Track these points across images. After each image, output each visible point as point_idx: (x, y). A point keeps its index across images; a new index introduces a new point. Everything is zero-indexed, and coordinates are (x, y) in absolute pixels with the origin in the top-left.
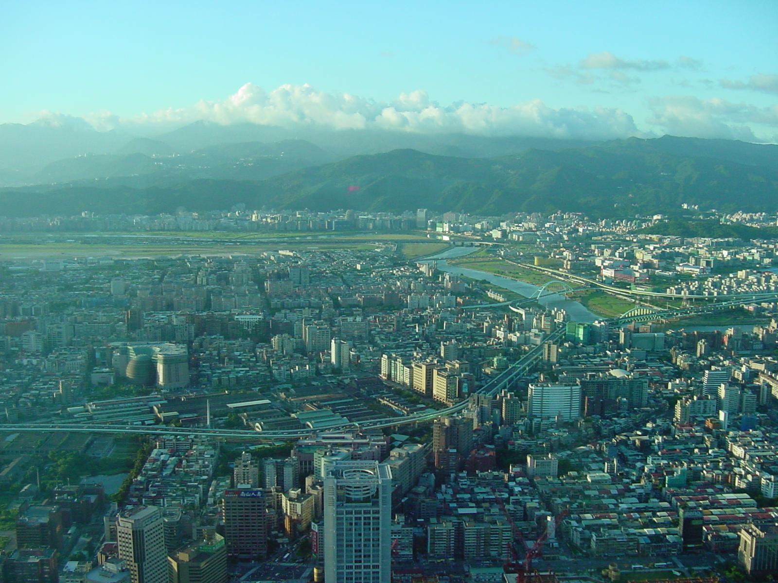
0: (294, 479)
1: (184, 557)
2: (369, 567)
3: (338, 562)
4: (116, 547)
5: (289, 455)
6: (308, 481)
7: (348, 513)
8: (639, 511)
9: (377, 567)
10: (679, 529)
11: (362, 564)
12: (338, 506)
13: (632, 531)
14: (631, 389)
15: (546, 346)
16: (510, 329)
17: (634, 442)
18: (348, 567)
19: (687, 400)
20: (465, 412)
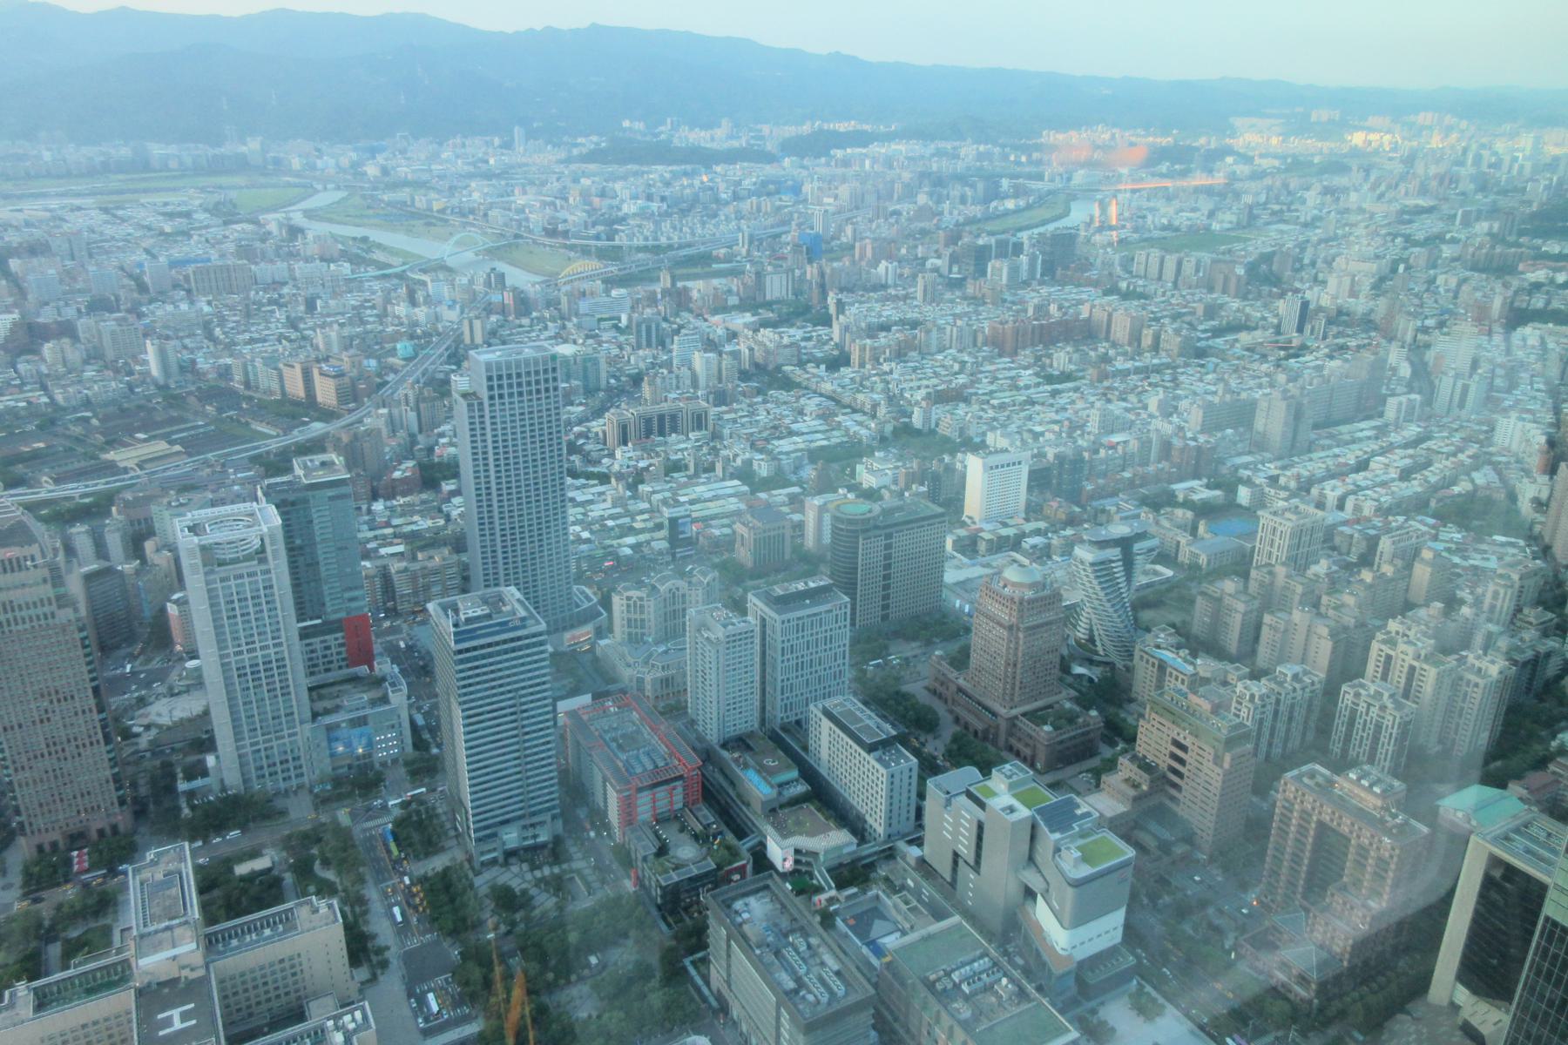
0: (125, 549)
2: (267, 647)
3: (220, 649)
5: (108, 514)
6: (149, 546)
7: (222, 580)
8: (612, 517)
9: (280, 644)
10: (664, 533)
11: (257, 645)
12: (206, 574)
13: (608, 542)
14: (585, 370)
15: (466, 323)
16: (413, 302)
18: (236, 654)
19: (656, 375)
20: (367, 421)
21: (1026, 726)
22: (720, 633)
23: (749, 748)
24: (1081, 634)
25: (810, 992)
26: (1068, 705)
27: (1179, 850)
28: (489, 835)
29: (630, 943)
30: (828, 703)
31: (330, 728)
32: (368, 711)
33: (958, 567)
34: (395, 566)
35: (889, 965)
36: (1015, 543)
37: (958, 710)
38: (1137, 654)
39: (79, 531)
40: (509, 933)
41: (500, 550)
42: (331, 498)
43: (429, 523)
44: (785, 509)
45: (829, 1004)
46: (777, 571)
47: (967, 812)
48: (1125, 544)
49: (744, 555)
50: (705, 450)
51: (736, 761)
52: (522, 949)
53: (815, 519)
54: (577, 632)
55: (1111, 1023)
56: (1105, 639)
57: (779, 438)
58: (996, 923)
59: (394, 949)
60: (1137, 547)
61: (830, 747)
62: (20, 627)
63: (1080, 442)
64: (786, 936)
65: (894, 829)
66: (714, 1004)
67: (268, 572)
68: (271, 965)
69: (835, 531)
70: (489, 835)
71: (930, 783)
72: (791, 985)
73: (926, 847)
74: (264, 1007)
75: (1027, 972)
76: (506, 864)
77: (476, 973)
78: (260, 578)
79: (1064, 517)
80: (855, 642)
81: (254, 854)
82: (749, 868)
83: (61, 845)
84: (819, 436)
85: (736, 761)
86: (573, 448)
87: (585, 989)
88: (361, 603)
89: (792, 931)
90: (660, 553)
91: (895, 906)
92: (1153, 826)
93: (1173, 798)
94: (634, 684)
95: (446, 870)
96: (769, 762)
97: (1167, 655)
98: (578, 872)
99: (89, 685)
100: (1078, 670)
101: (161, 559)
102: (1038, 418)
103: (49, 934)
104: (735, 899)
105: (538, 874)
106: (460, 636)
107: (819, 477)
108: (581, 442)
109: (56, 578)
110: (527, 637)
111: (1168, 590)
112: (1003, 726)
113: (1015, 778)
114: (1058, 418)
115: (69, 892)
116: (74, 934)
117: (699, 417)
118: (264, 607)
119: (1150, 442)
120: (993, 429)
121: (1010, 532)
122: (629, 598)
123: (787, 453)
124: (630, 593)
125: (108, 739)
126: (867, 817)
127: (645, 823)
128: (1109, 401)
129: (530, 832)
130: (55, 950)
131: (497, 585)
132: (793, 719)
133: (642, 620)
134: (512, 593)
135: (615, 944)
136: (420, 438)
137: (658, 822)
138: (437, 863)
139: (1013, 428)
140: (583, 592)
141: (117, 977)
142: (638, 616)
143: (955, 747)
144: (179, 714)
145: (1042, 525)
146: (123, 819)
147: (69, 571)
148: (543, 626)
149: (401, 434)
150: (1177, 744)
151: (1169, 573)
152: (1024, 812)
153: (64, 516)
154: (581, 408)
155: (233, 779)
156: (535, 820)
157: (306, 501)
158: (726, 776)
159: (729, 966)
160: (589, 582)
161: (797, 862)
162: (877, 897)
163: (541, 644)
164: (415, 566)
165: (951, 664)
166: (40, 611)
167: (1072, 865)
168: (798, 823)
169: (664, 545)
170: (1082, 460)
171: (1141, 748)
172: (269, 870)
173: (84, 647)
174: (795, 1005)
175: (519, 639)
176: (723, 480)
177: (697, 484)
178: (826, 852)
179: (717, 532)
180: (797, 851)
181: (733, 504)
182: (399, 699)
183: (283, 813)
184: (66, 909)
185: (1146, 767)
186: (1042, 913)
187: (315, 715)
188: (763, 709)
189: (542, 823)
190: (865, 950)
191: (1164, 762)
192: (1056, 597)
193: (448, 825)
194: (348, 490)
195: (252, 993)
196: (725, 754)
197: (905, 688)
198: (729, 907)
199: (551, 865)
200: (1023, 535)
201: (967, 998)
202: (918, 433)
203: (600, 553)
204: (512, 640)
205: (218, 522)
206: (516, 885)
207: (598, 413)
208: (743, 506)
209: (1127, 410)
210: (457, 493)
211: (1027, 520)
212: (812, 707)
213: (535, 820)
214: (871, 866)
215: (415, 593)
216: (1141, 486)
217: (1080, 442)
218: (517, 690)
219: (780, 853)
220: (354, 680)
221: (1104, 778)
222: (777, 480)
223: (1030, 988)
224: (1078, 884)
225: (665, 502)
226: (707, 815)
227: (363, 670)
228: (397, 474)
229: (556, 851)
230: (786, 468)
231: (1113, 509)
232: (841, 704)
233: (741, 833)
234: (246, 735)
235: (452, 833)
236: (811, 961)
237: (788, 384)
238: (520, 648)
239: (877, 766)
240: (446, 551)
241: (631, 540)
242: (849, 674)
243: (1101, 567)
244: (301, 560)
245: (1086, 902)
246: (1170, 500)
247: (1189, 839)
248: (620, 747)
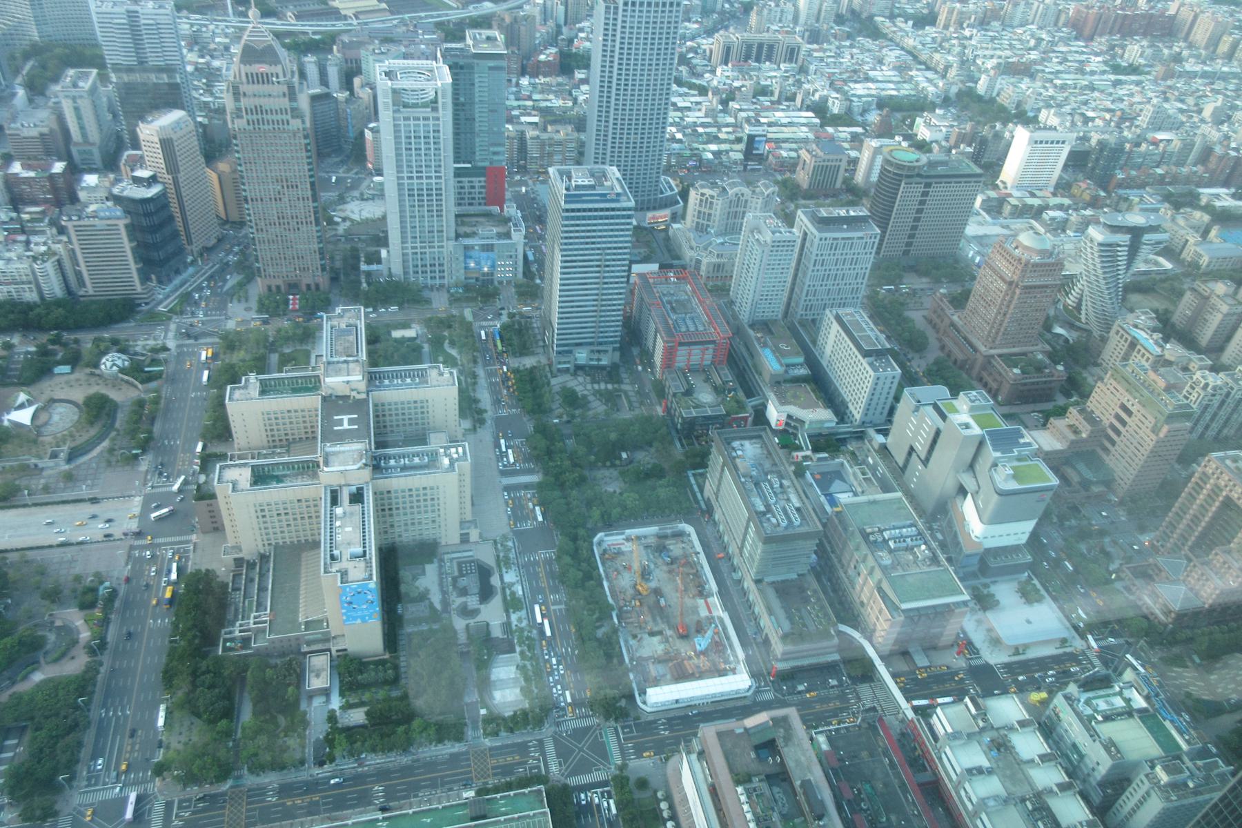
0: (341, 82)
1: (223, 166)
2: (430, 178)
4: (142, 157)
5: (331, 51)
6: (357, 81)
7: (406, 119)
8: (703, 125)
9: (440, 177)
10: (742, 146)
11: (424, 175)
12: (394, 112)
13: (696, 145)
17: (705, 51)
19: (764, 6)
20: (526, 7)
21: (999, 364)
22: (768, 237)
23: (771, 332)
24: (1071, 301)
25: (774, 516)
26: (1040, 356)
27: (1096, 489)
28: (566, 350)
29: (653, 450)
30: (841, 311)
31: (467, 248)
32: (495, 242)
33: (980, 224)
34: (531, 133)
35: (838, 513)
36: (1037, 213)
37: (947, 340)
38: (1115, 328)
39: (310, 60)
40: (569, 422)
41: (610, 136)
42: (490, 68)
43: (561, 102)
44: (846, 145)
45: (786, 528)
46: (826, 196)
47: (930, 419)
48: (1136, 233)
49: (802, 178)
50: (791, 81)
51: (758, 339)
52: (577, 435)
53: (868, 159)
54: (658, 213)
55: (998, 597)
56: (1090, 309)
57: (856, 82)
58: (929, 505)
59: (490, 413)
60: (1147, 237)
61: (834, 344)
62: (266, 127)
63: (1125, 133)
64: (766, 474)
65: (868, 419)
66: (703, 506)
67: (438, 119)
68: (409, 403)
69: (883, 171)
70: (566, 350)
71: (907, 391)
72: (762, 508)
73: (890, 439)
74: (401, 429)
75: (943, 546)
76: (575, 374)
77: (543, 443)
78: (431, 122)
79: (1086, 197)
80: (876, 267)
81: (405, 326)
82: (750, 420)
83: (283, 288)
84: (892, 86)
85: (758, 339)
86: (683, 60)
87: (615, 473)
88: (501, 158)
89: (772, 472)
90: (735, 163)
91: (854, 474)
92: (1081, 467)
93: (1106, 450)
94: (693, 263)
95: (535, 367)
96: (783, 346)
97: (1142, 335)
98: (626, 393)
99: (308, 180)
100: (1059, 330)
101: (364, 94)
102: (1093, 104)
103: (272, 347)
104: (735, 439)
105: (596, 386)
106: (569, 198)
107: (882, 122)
108: (691, 55)
109: (292, 94)
110: (619, 210)
111: (1163, 281)
112: (980, 360)
113: (977, 403)
114: (1113, 107)
115: (285, 324)
116: (287, 351)
117: (793, 50)
118: (432, 146)
119: (1193, 145)
120: (1049, 106)
121: (1036, 202)
122: (703, 195)
123: (860, 97)
124: (705, 191)
125: (317, 223)
126: (850, 405)
127: (682, 371)
128: (1166, 100)
129: (596, 356)
130: (274, 358)
131: (603, 163)
132: (810, 318)
133: (710, 215)
134: (614, 172)
135: (641, 448)
136: (564, 30)
137: (690, 371)
138: (528, 362)
139: (1067, 109)
140: (668, 183)
141: (311, 385)
142: (707, 211)
143: (935, 368)
144: (366, 215)
145: (1066, 201)
146: (323, 280)
147: (301, 91)
148: (632, 204)
149: (551, 23)
150: (1124, 408)
151: (1168, 265)
152: (977, 430)
153: (302, 47)
154: (696, 26)
155: (397, 269)
156: (600, 348)
157: (471, 67)
158: (748, 349)
159: (720, 483)
160: (674, 175)
161: (787, 424)
162: (842, 464)
163: (629, 217)
164: (545, 136)
165: (951, 302)
166: (279, 117)
167: (1004, 479)
168: (795, 397)
169: (740, 156)
170: (1122, 150)
171: (1091, 404)
172: (414, 339)
173: (307, 151)
174: (761, 522)
175: (613, 209)
176: (800, 110)
177: (778, 110)
178: (811, 422)
179: (784, 154)
180: (789, 417)
181: (803, 132)
182: (518, 237)
183: (428, 301)
184: (283, 333)
185: (1090, 418)
186: (968, 507)
187: (458, 236)
188: (788, 304)
189: (606, 351)
190: (823, 498)
191: (1107, 419)
192: (1060, 265)
193: (539, 337)
194: (504, 63)
195: (394, 418)
196: (751, 332)
197: (907, 314)
198: (729, 444)
199: (606, 383)
200: (1047, 207)
201: (891, 551)
202: (980, 98)
203: (688, 152)
204: (607, 210)
205: (406, 72)
206: (578, 389)
207: (709, 33)
208: (811, 136)
209: (1181, 111)
210: (585, 81)
211: (1054, 194)
212: (827, 311)
213: (600, 348)
214: (843, 441)
215: (542, 157)
216: (1170, 184)
217: (1125, 133)
218: (604, 249)
219: (775, 414)
220: (488, 215)
221: (1052, 419)
222: (845, 119)
223: (942, 557)
224: (1002, 493)
225: (748, 120)
226: (728, 375)
227: (496, 209)
228: (542, 57)
229: (612, 374)
230: (856, 109)
231: (1137, 199)
232: (851, 315)
233: (750, 393)
234: (409, 240)
235: (541, 343)
236: (780, 496)
237: (875, 33)
238: (612, 217)
239: (868, 368)
240: (569, 128)
241: (714, 147)
242: (863, 292)
243: (1108, 249)
244: (462, 114)
245: (1006, 507)
246: (1191, 200)
247: (1109, 483)
248: (673, 309)
